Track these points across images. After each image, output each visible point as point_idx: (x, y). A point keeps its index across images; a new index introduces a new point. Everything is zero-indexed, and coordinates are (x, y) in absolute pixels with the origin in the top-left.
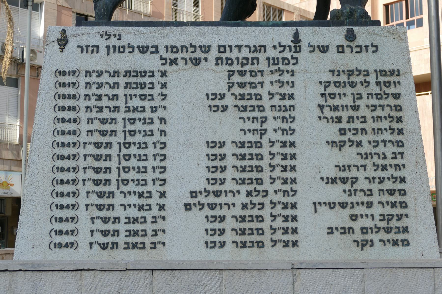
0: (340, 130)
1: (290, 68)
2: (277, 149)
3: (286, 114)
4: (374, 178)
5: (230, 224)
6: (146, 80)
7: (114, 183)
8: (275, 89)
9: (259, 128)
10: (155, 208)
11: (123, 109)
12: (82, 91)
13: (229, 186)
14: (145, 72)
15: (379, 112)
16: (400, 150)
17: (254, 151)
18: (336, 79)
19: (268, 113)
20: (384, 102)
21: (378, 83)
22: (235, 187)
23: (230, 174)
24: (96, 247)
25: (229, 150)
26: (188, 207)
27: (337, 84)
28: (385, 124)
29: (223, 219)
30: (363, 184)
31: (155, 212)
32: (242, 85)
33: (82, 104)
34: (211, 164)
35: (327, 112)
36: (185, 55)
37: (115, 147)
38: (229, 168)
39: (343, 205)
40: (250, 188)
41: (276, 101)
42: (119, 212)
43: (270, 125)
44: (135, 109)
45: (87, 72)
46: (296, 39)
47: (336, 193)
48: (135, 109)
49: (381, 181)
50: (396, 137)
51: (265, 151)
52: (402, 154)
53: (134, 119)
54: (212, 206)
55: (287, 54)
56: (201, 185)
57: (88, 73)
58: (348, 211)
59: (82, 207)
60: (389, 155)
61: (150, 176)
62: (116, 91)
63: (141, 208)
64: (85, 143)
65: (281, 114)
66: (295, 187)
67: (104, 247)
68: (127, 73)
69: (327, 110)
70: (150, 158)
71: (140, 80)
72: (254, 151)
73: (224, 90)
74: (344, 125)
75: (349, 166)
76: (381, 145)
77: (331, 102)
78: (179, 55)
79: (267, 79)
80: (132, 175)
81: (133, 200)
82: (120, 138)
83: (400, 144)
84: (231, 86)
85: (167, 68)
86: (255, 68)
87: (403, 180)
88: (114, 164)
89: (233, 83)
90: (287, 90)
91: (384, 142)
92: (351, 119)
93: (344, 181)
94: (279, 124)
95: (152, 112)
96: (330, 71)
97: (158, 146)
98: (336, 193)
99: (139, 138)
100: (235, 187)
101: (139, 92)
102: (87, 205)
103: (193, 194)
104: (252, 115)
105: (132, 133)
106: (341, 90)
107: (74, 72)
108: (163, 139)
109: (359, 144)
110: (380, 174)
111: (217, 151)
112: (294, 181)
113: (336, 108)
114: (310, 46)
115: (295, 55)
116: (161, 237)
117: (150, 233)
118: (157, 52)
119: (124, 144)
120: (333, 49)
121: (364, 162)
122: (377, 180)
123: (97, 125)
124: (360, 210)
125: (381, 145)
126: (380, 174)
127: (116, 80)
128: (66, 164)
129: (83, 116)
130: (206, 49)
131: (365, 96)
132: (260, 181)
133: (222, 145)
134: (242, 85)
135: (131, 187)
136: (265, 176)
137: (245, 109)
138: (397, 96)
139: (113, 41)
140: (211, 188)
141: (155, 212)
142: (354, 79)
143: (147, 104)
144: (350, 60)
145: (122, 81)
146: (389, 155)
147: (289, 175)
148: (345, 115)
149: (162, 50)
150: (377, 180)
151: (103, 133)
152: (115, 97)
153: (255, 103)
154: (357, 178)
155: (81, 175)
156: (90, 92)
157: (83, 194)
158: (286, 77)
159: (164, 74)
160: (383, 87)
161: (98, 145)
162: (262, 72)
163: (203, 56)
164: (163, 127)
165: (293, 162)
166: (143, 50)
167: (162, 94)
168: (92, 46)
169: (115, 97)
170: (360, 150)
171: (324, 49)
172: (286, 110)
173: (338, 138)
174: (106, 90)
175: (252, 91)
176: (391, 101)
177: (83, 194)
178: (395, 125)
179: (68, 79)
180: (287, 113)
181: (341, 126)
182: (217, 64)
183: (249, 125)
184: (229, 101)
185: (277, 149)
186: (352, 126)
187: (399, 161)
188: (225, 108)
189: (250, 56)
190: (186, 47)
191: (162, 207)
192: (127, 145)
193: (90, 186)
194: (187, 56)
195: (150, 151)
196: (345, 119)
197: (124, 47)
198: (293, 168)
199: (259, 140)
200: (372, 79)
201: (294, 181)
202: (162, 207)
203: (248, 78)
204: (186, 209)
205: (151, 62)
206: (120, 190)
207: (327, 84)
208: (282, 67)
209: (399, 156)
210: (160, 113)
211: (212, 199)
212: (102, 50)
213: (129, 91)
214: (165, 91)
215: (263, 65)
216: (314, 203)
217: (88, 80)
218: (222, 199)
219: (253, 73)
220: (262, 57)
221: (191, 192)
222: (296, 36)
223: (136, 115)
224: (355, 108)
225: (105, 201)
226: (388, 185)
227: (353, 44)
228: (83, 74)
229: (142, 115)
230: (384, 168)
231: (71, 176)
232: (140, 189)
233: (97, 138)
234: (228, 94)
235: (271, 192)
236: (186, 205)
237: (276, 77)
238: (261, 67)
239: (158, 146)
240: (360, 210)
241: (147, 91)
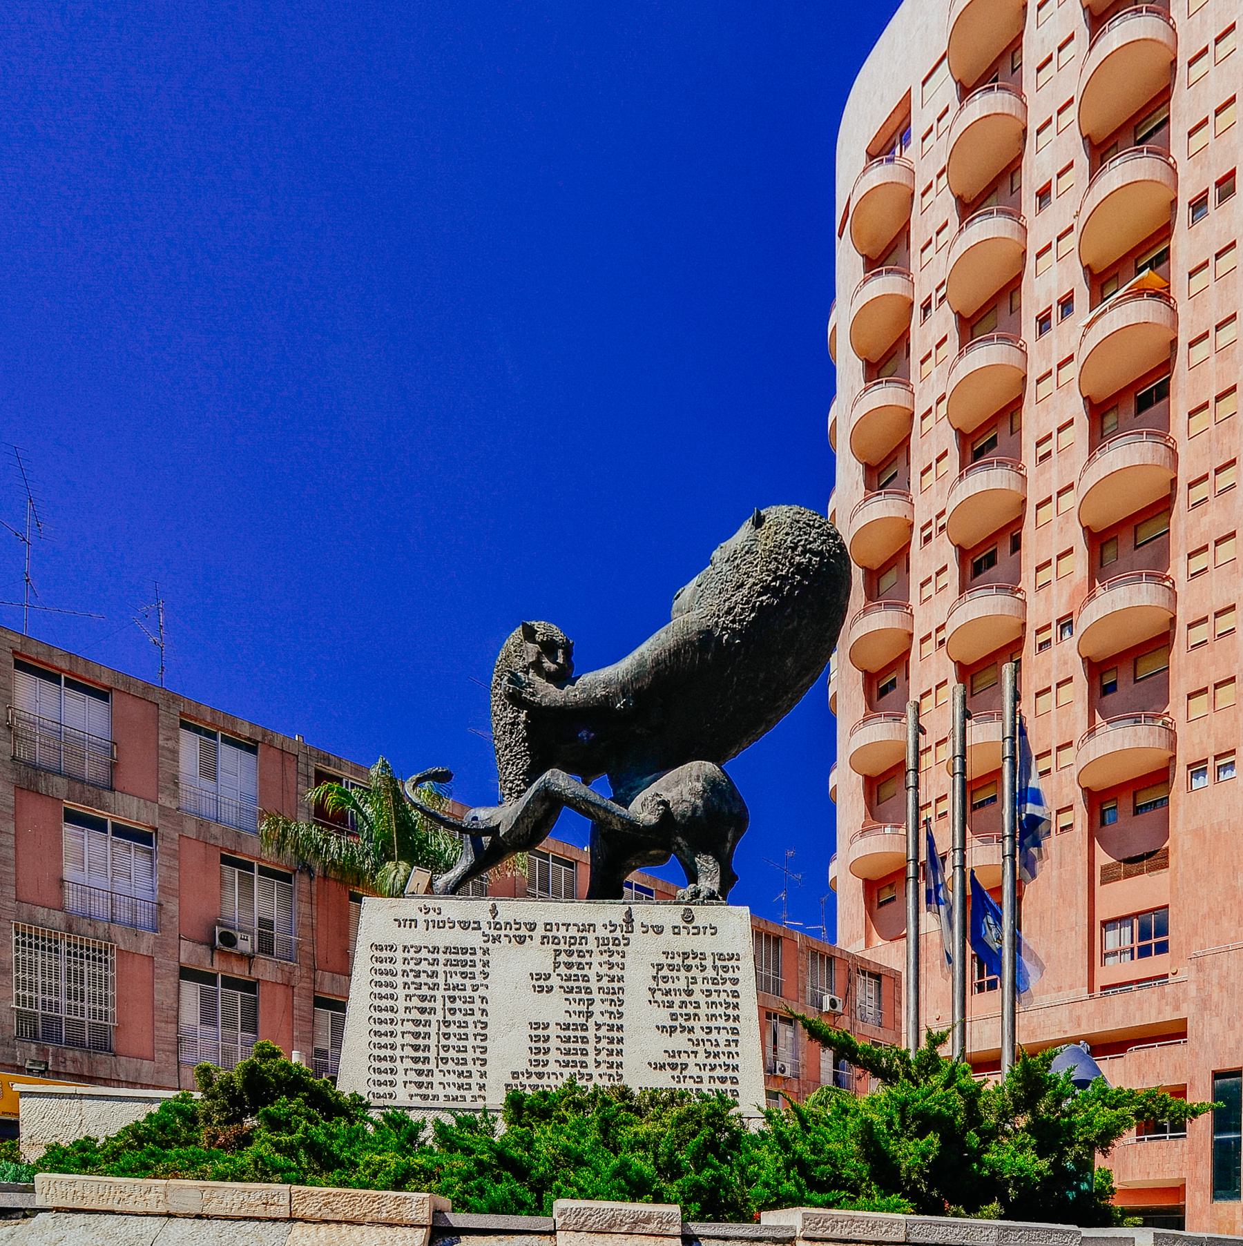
0: (672, 1015)
1: (620, 949)
2: (603, 1032)
3: (615, 998)
4: (705, 1065)
6: (468, 957)
7: (433, 1061)
8: (604, 970)
10: (475, 1088)
11: (442, 987)
12: (399, 966)
15: (714, 998)
16: (735, 1037)
17: (579, 1033)
18: (670, 961)
19: (596, 996)
20: (720, 987)
21: (715, 967)
22: (558, 1070)
23: (554, 1055)
25: (553, 1031)
27: (671, 967)
28: (720, 1010)
30: (693, 1071)
31: (475, 1091)
32: (569, 966)
33: (399, 980)
34: (533, 1045)
35: (658, 996)
36: (508, 932)
37: (434, 1025)
38: (553, 1050)
41: (604, 983)
42: (438, 1090)
43: (597, 1008)
44: (456, 987)
46: (629, 919)
48: (456, 987)
49: (713, 1068)
50: (730, 1024)
51: (590, 1034)
52: (736, 1041)
55: (618, 934)
56: (523, 1066)
59: (400, 1084)
60: (722, 1043)
61: (470, 1055)
62: (435, 968)
63: (460, 1087)
65: (610, 997)
66: (620, 1071)
69: (658, 996)
70: (471, 1037)
71: (460, 957)
72: (579, 1033)
74: (676, 1009)
75: (680, 1052)
76: (715, 1032)
77: (662, 985)
78: (503, 932)
79: (596, 959)
80: (452, 1054)
81: (452, 1078)
82: (439, 1015)
83: (735, 1031)
84: (557, 965)
85: (489, 945)
86: (584, 948)
87: (735, 1068)
88: (432, 1042)
90: (616, 972)
91: (718, 1029)
92: (683, 1004)
93: (674, 1067)
94: (606, 1006)
97: (479, 1025)
99: (459, 1017)
100: (558, 1070)
101: (459, 969)
102: (405, 1083)
103: (515, 1075)
104: (578, 996)
105: (453, 1011)
106: (675, 974)
108: (484, 1019)
109: (691, 1030)
110: (711, 1060)
111: (540, 1032)
112: (620, 1065)
113: (668, 993)
114: (643, 926)
115: (627, 935)
119: (444, 1022)
120: (668, 930)
121: (695, 1048)
122: (708, 1068)
123: (415, 1002)
125: (715, 1032)
126: (711, 1060)
127: (435, 956)
128: (384, 1040)
129: (400, 992)
130: (532, 927)
131: (700, 980)
132: (584, 1065)
133: (546, 1026)
134: (569, 966)
135: (451, 1066)
136: (590, 1060)
137: (571, 991)
138: (735, 981)
139: (432, 916)
140: (532, 1069)
142: (689, 962)
143: (468, 982)
144: (686, 942)
145: (442, 957)
146: (722, 1043)
148: (677, 1000)
149: (484, 926)
150: (708, 1068)
151: (422, 1011)
152: (434, 974)
153: (581, 984)
154: (687, 1065)
155: (398, 1053)
156: (408, 968)
157: (401, 1072)
158: (616, 959)
159: (486, 952)
160: (721, 972)
161: (417, 1023)
162: (590, 952)
163: (528, 934)
164: (484, 1006)
165: (620, 1047)
166: (465, 925)
167: (483, 972)
169: (434, 974)
170: (691, 1036)
171: (659, 930)
172: (614, 993)
173: (669, 1023)
174: (424, 966)
175: (580, 972)
177: (401, 1072)
178: (730, 1012)
180: (615, 996)
181: (671, 1010)
182: (543, 943)
183: (575, 1007)
184: (555, 981)
186: (684, 1011)
187: (733, 1049)
189: (579, 935)
192: (447, 1024)
193: (408, 1064)
195: (471, 1030)
196: (677, 1004)
197: (443, 922)
198: (620, 1053)
200: (708, 963)
201: (620, 1065)
202: (482, 1087)
203: (575, 959)
205: (473, 939)
207: (660, 967)
209: (733, 1044)
210: (482, 991)
213: (448, 969)
214: (486, 970)
215: (592, 945)
217: (406, 955)
219: (581, 954)
220: (591, 936)
221: (513, 1073)
222: (629, 913)
223: (457, 993)
224: (689, 993)
225: (423, 1079)
226: (719, 1072)
227: (690, 926)
228: (400, 948)
229: (462, 994)
230: (716, 1055)
231: (389, 1052)
232: (460, 1068)
233: (415, 1015)
234: (554, 975)
235: (595, 1076)
237: (605, 957)
238: (588, 947)
239: (479, 1025)
241: (468, 969)
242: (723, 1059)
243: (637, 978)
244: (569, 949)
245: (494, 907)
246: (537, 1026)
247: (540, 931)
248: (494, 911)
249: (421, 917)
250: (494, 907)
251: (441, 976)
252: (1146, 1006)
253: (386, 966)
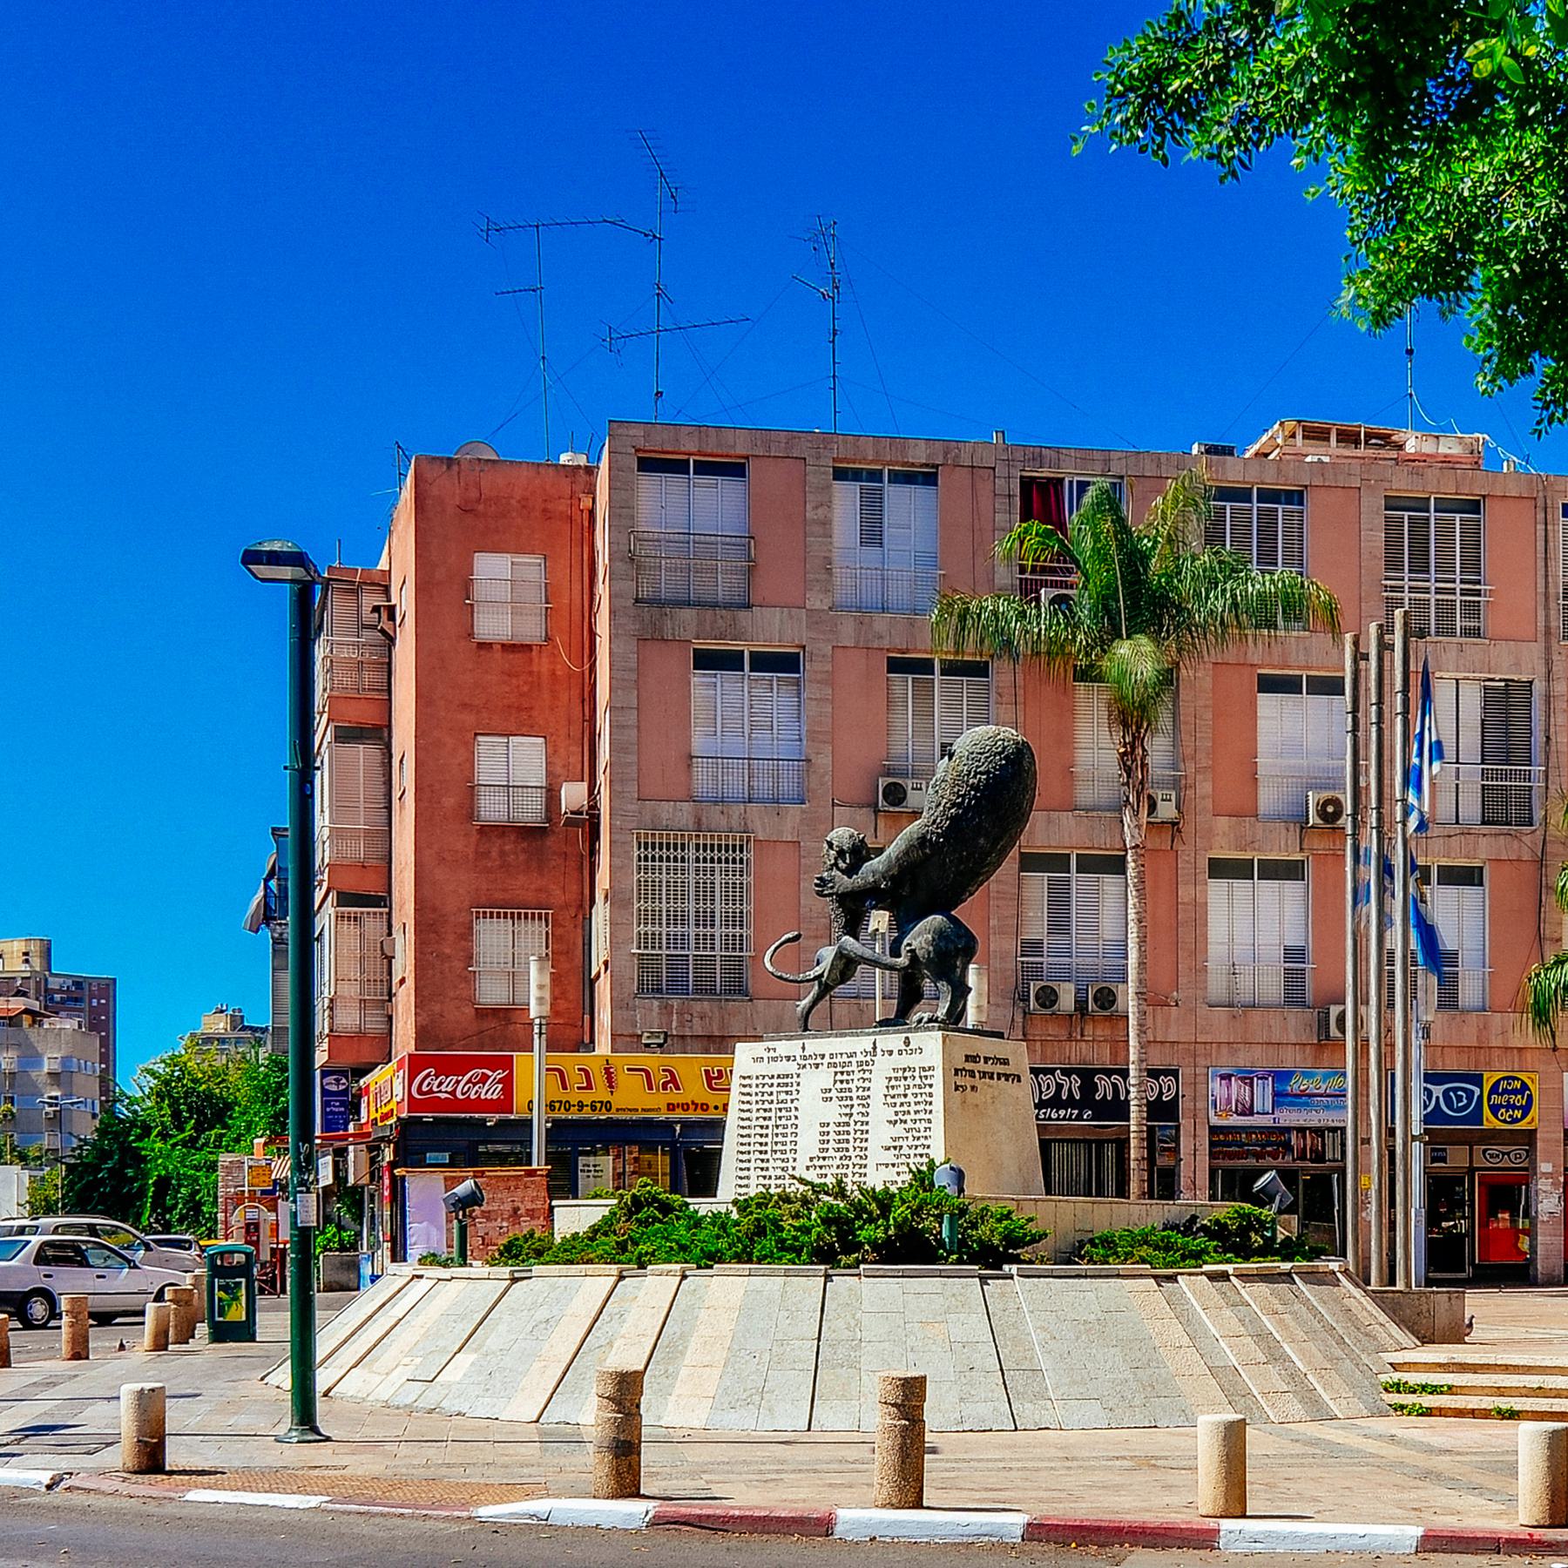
13: (831, 1153)
23: (832, 1144)
30: (905, 1151)
35: (889, 1100)
42: (771, 1172)
47: (889, 1157)
50: (928, 1116)
56: (816, 1153)
74: (898, 1108)
81: (779, 1163)
83: (929, 1121)
90: (867, 1084)
98: (889, 1157)
103: (811, 1159)
123: (762, 1113)
128: (746, 1140)
130: (823, 1056)
139: (772, 1054)
144: (906, 1060)
145: (775, 1081)
147: (864, 1145)
158: (867, 1075)
166: (788, 1058)
176: (927, 1090)
179: (747, 1082)
184: (834, 1094)
185: (858, 1127)
203: (845, 1077)
205: (791, 1067)
207: (890, 1079)
211: (821, 1162)
215: (854, 1067)
218: (826, 1163)
220: (853, 1060)
226: (920, 1150)
242: (922, 1141)
243: (878, 1087)
244: (841, 1070)
246: (823, 1125)
249: (765, 1055)
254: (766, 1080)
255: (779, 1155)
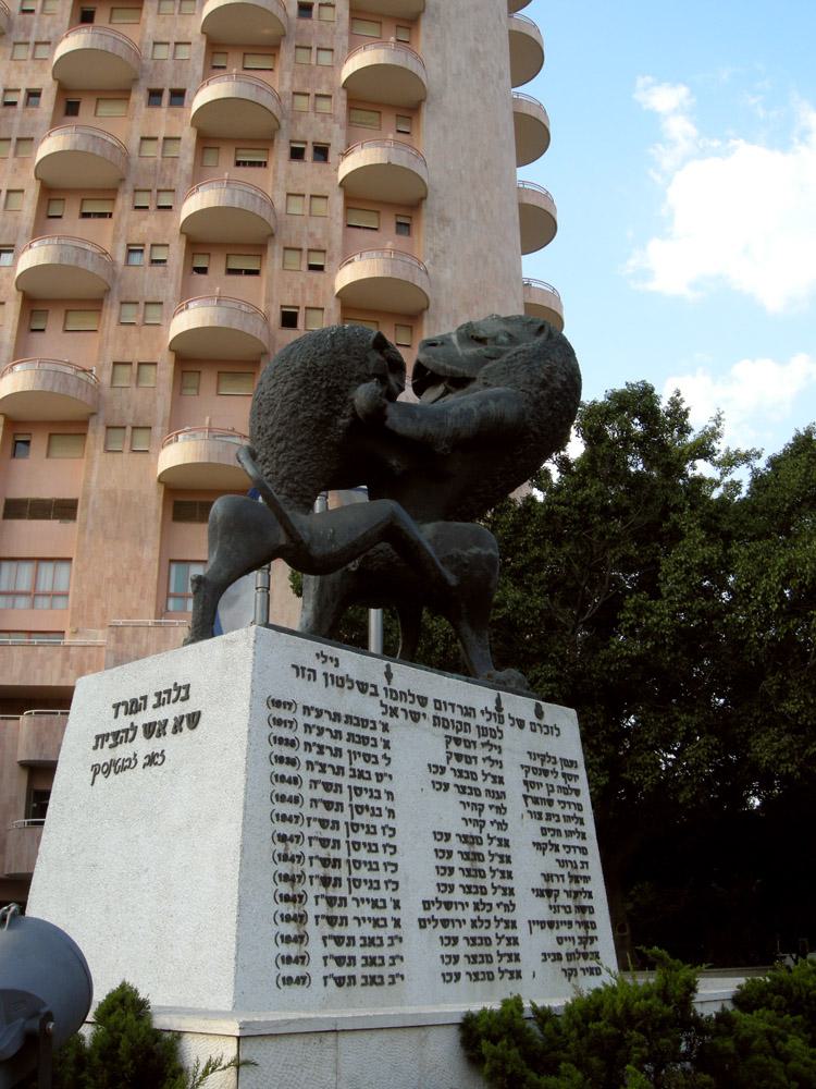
5: (462, 949)
9: (478, 818)
11: (348, 772)
13: (458, 895)
14: (367, 721)
21: (564, 775)
24: (331, 982)
26: (423, 923)
29: (455, 940)
32: (459, 757)
39: (551, 924)
40: (477, 898)
45: (305, 708)
46: (499, 708)
53: (360, 789)
54: (445, 923)
55: (493, 724)
56: (432, 893)
57: (307, 710)
58: (556, 933)
64: (309, 819)
67: (340, 981)
68: (349, 719)
69: (529, 801)
73: (444, 764)
78: (399, 704)
81: (367, 911)
89: (451, 753)
93: (549, 893)
95: (378, 781)
96: (529, 753)
97: (388, 832)
103: (427, 905)
107: (290, 704)
116: (399, 968)
117: (388, 961)
118: (375, 694)
123: (320, 793)
124: (564, 931)
130: (423, 701)
134: (459, 757)
139: (330, 668)
141: (391, 930)
143: (373, 769)
145: (345, 729)
158: (494, 755)
159: (385, 728)
166: (363, 687)
168: (309, 670)
171: (521, 724)
173: (542, 840)
179: (283, 714)
188: (447, 786)
190: (405, 694)
191: (397, 923)
194: (408, 707)
197: (342, 678)
199: (478, 834)
203: (462, 750)
204: (421, 927)
206: (352, 895)
208: (492, 741)
210: (384, 786)
211: (442, 914)
212: (320, 676)
216: (529, 922)
221: (424, 902)
222: (498, 701)
228: (300, 709)
233: (321, 812)
236: (420, 920)
240: (564, 931)
245: (388, 666)
247: (430, 710)
248: (389, 675)
250: (388, 666)
251: (346, 756)
252: (48, 664)
253: (285, 733)
254: (325, 722)
255: (364, 892)
